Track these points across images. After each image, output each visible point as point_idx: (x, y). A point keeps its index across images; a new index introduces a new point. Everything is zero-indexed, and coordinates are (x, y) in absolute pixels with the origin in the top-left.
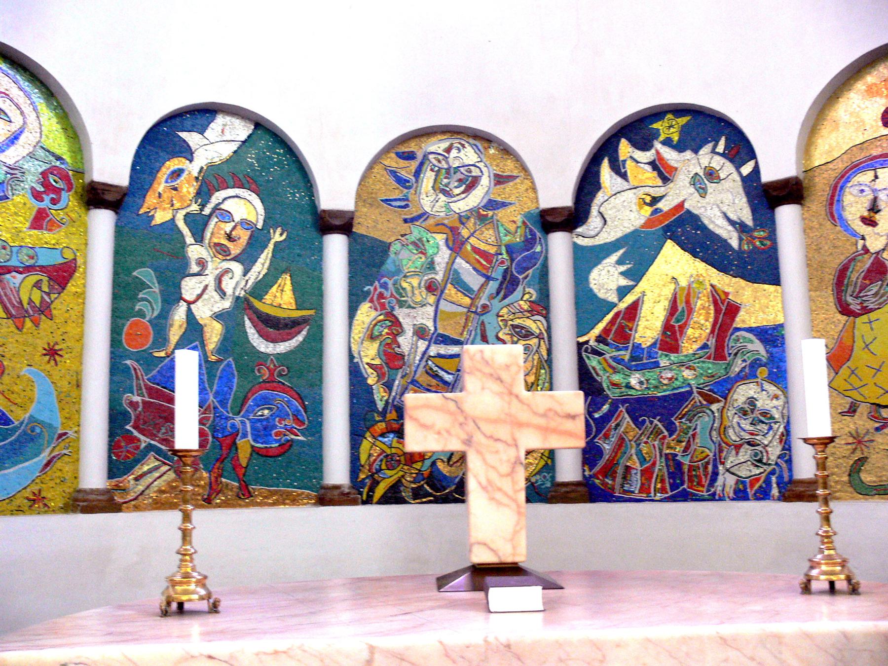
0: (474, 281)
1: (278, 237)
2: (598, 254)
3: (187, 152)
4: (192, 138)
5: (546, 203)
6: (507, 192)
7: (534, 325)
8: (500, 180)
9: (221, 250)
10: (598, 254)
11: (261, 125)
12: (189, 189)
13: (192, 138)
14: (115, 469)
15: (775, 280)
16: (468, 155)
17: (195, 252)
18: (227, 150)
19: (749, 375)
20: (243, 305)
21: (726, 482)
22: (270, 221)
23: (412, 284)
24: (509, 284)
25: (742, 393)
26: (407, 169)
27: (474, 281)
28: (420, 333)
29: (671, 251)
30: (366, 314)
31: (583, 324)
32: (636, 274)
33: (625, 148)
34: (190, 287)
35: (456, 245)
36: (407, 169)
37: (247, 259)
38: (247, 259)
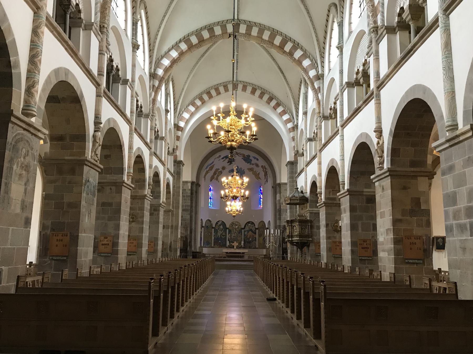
0: (237, 233)
1: (224, 229)
2: (246, 231)
3: (218, 224)
4: (218, 223)
5: (242, 227)
6: (240, 226)
7: (241, 236)
8: (239, 225)
9: (220, 231)
10: (246, 231)
11: (222, 221)
12: (218, 226)
13: (218, 223)
14: (214, 245)
15: (256, 234)
16: (237, 223)
17: (218, 231)
18: (220, 223)
19: (254, 241)
20: (221, 234)
21: (253, 248)
22: (223, 228)
23: (233, 233)
24: (239, 233)
25: (254, 242)
26: (232, 224)
27: (237, 233)
28: (233, 236)
29: (250, 232)
30: (229, 235)
31: (244, 236)
32: (248, 233)
33: (248, 224)
34: (218, 233)
35: (236, 230)
36: (232, 224)
37: (222, 231)
38: (222, 231)
